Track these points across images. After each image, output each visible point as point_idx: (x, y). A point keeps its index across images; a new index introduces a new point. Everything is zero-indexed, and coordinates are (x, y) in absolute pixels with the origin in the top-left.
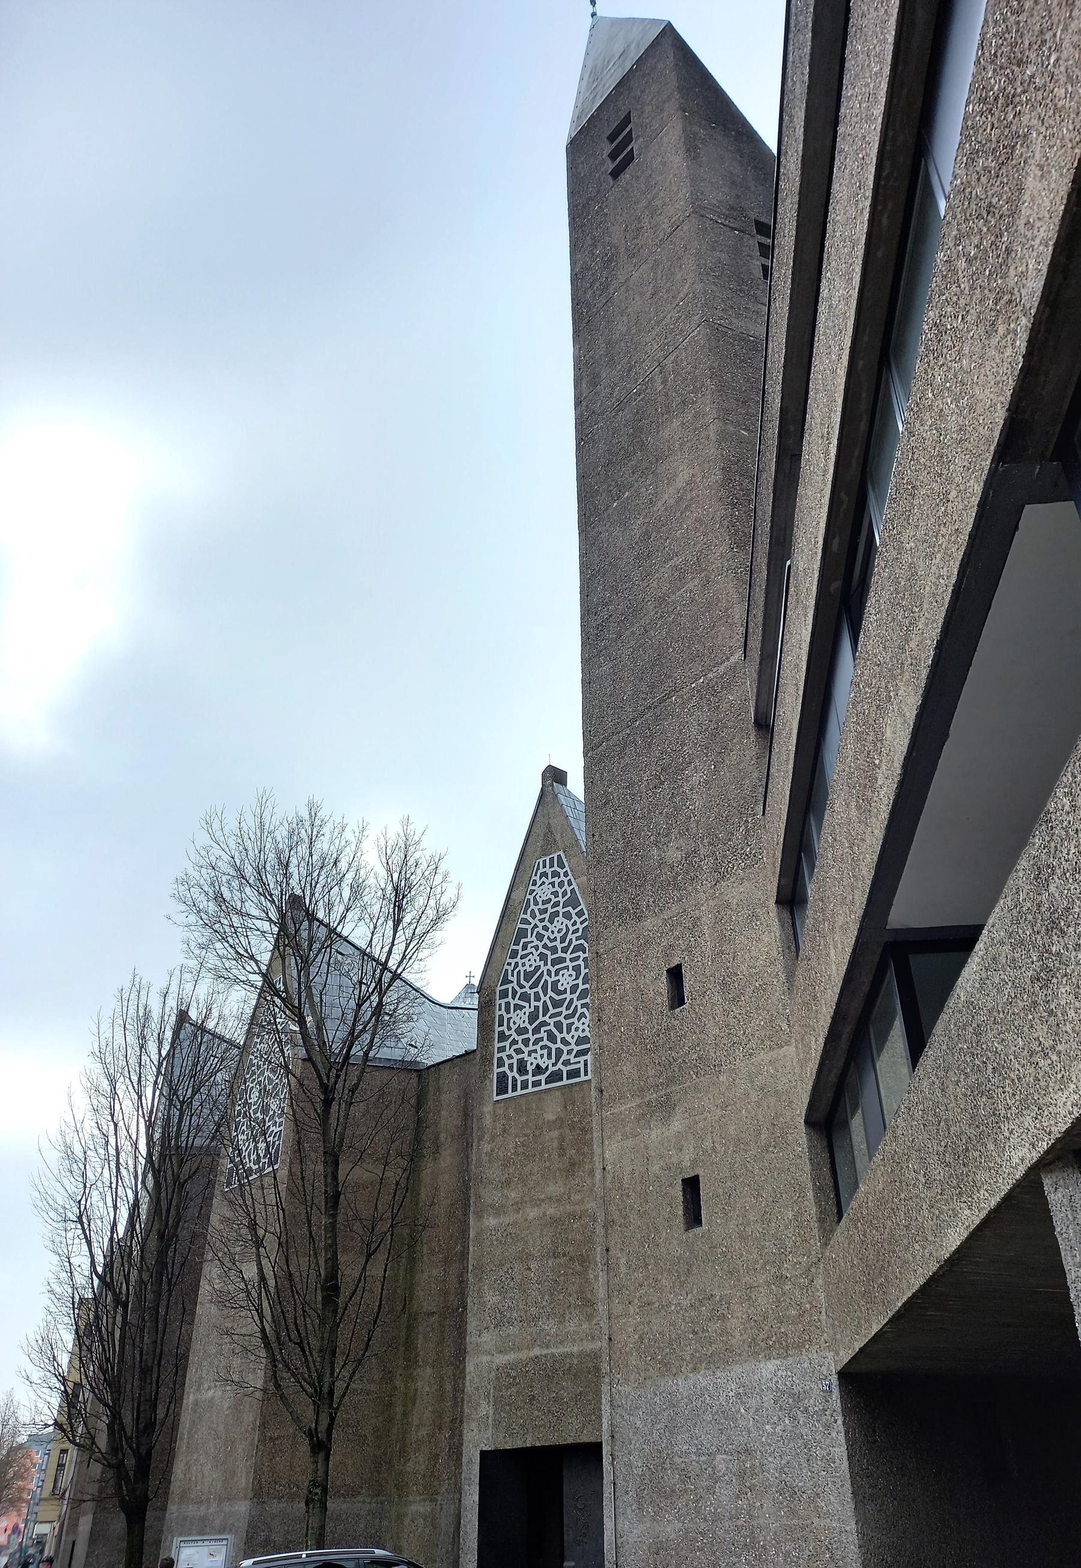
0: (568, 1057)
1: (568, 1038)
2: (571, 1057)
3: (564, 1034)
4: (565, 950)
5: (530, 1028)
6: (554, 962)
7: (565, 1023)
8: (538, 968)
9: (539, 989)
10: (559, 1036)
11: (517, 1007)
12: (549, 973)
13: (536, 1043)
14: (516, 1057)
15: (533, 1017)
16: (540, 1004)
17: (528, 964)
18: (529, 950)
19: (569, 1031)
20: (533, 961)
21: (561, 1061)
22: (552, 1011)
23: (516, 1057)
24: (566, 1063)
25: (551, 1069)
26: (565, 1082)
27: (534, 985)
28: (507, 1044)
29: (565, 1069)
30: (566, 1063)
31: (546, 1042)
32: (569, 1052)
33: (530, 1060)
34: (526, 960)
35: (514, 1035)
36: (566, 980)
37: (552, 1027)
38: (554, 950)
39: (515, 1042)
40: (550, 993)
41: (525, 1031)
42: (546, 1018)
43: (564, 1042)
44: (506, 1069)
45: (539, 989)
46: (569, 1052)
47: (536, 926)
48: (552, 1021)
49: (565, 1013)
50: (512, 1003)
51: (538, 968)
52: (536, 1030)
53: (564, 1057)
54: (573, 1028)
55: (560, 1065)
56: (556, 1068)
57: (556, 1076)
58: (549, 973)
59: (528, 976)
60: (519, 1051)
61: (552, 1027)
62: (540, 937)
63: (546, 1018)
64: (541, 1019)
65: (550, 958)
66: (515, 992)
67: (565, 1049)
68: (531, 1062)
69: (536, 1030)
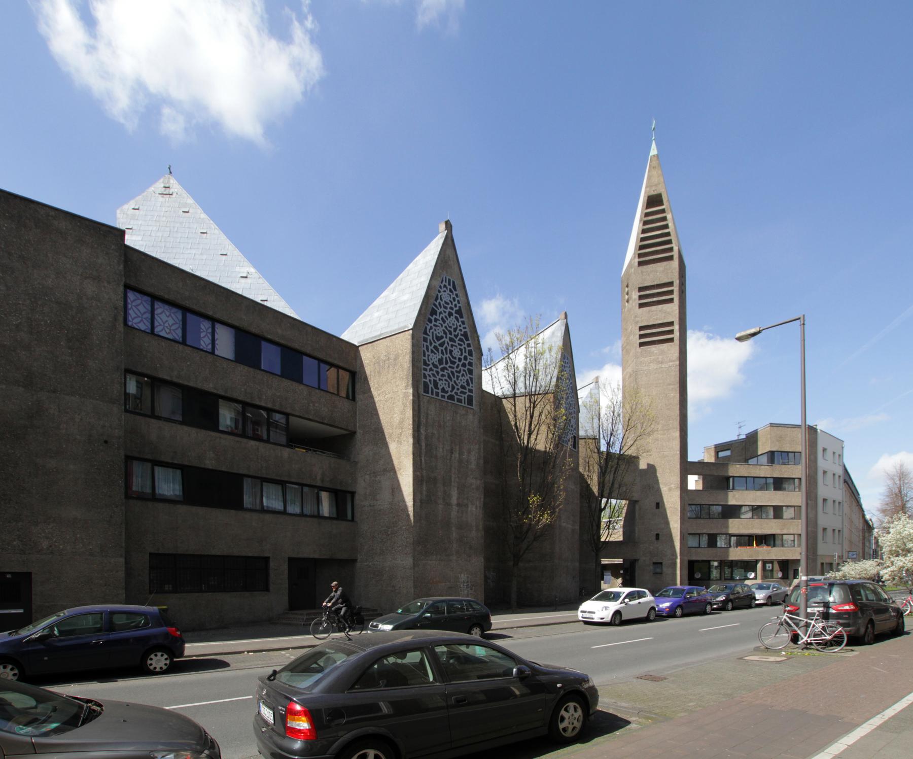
4: (456, 336)
5: (440, 367)
6: (451, 340)
8: (442, 337)
11: (432, 351)
13: (443, 376)
14: (432, 378)
15: (441, 361)
20: (439, 332)
23: (432, 378)
25: (450, 393)
26: (455, 402)
28: (428, 368)
31: (446, 378)
33: (440, 383)
35: (431, 366)
36: (456, 353)
38: (451, 333)
39: (431, 369)
41: (436, 366)
44: (427, 381)
47: (441, 313)
50: (430, 348)
51: (442, 337)
52: (443, 369)
53: (455, 390)
57: (451, 397)
59: (439, 338)
60: (434, 375)
62: (444, 322)
64: (444, 365)
65: (449, 336)
66: (431, 344)
68: (441, 384)
69: (443, 369)
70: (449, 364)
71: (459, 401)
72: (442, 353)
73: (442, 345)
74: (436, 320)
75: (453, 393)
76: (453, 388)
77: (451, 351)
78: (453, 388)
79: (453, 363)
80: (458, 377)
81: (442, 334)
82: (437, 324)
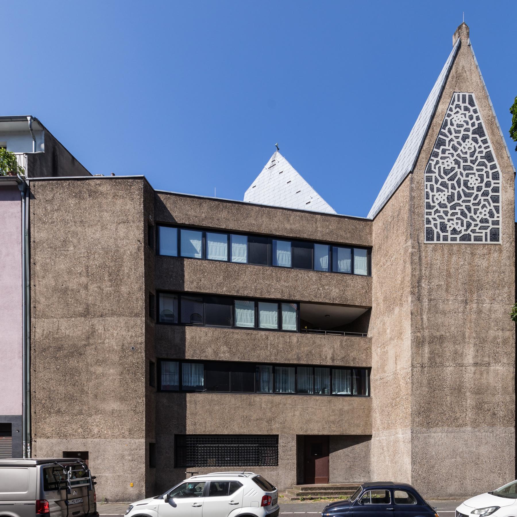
0: (475, 228)
1: (475, 217)
2: (477, 228)
3: (472, 214)
7: (473, 208)
8: (453, 169)
9: (455, 182)
10: (469, 215)
12: (461, 174)
16: (456, 192)
17: (446, 164)
18: (446, 155)
19: (475, 213)
20: (450, 163)
21: (470, 229)
22: (463, 198)
24: (473, 231)
26: (472, 242)
27: (451, 179)
29: (473, 235)
30: (473, 231)
32: (476, 225)
34: (445, 161)
37: (463, 208)
40: (462, 187)
42: (460, 202)
43: (471, 218)
45: (455, 182)
46: (476, 225)
48: (464, 204)
49: (472, 202)
53: (472, 227)
54: (478, 212)
55: (469, 232)
56: (467, 233)
58: (461, 174)
59: (446, 172)
61: (463, 208)
63: (460, 202)
64: (456, 201)
67: (473, 223)
70: (463, 198)
71: (477, 239)
72: (453, 187)
73: (451, 179)
74: (444, 151)
75: (469, 232)
76: (469, 225)
77: (466, 183)
78: (469, 225)
79: (470, 195)
80: (476, 211)
81: (453, 165)
82: (446, 155)
